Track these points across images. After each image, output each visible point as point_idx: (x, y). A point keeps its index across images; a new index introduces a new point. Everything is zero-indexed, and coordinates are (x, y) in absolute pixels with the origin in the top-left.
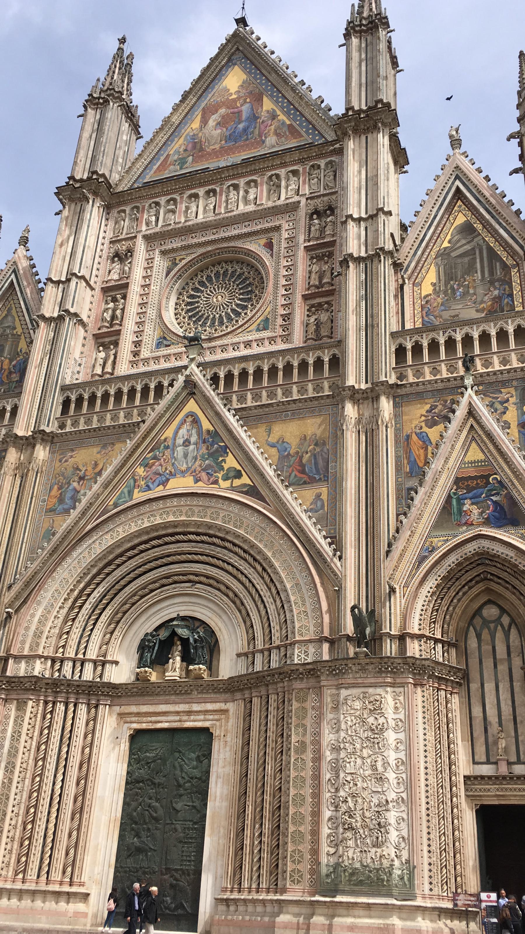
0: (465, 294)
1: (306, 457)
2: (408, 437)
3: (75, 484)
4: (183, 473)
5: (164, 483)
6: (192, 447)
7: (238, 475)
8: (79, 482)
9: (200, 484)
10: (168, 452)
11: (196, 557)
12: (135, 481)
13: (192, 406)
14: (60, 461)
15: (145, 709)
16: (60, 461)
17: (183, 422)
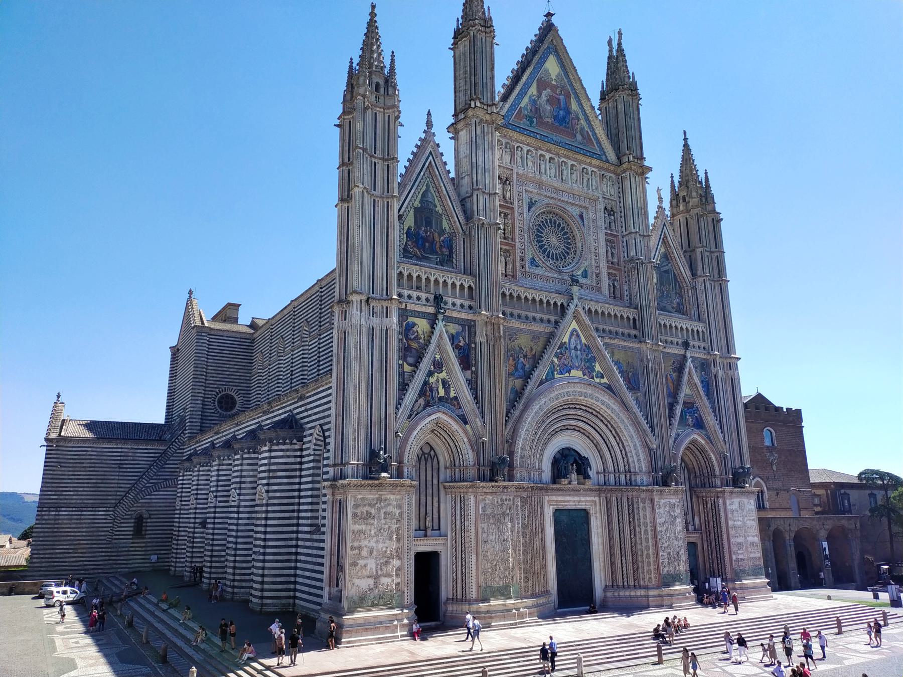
0: (667, 295)
1: (630, 374)
2: (667, 376)
3: (522, 359)
4: (577, 368)
5: (569, 372)
6: (579, 352)
7: (603, 378)
8: (524, 359)
9: (585, 377)
10: (567, 351)
11: (581, 418)
12: (554, 366)
13: (574, 325)
14: (510, 340)
15: (560, 498)
16: (510, 340)
17: (572, 334)
